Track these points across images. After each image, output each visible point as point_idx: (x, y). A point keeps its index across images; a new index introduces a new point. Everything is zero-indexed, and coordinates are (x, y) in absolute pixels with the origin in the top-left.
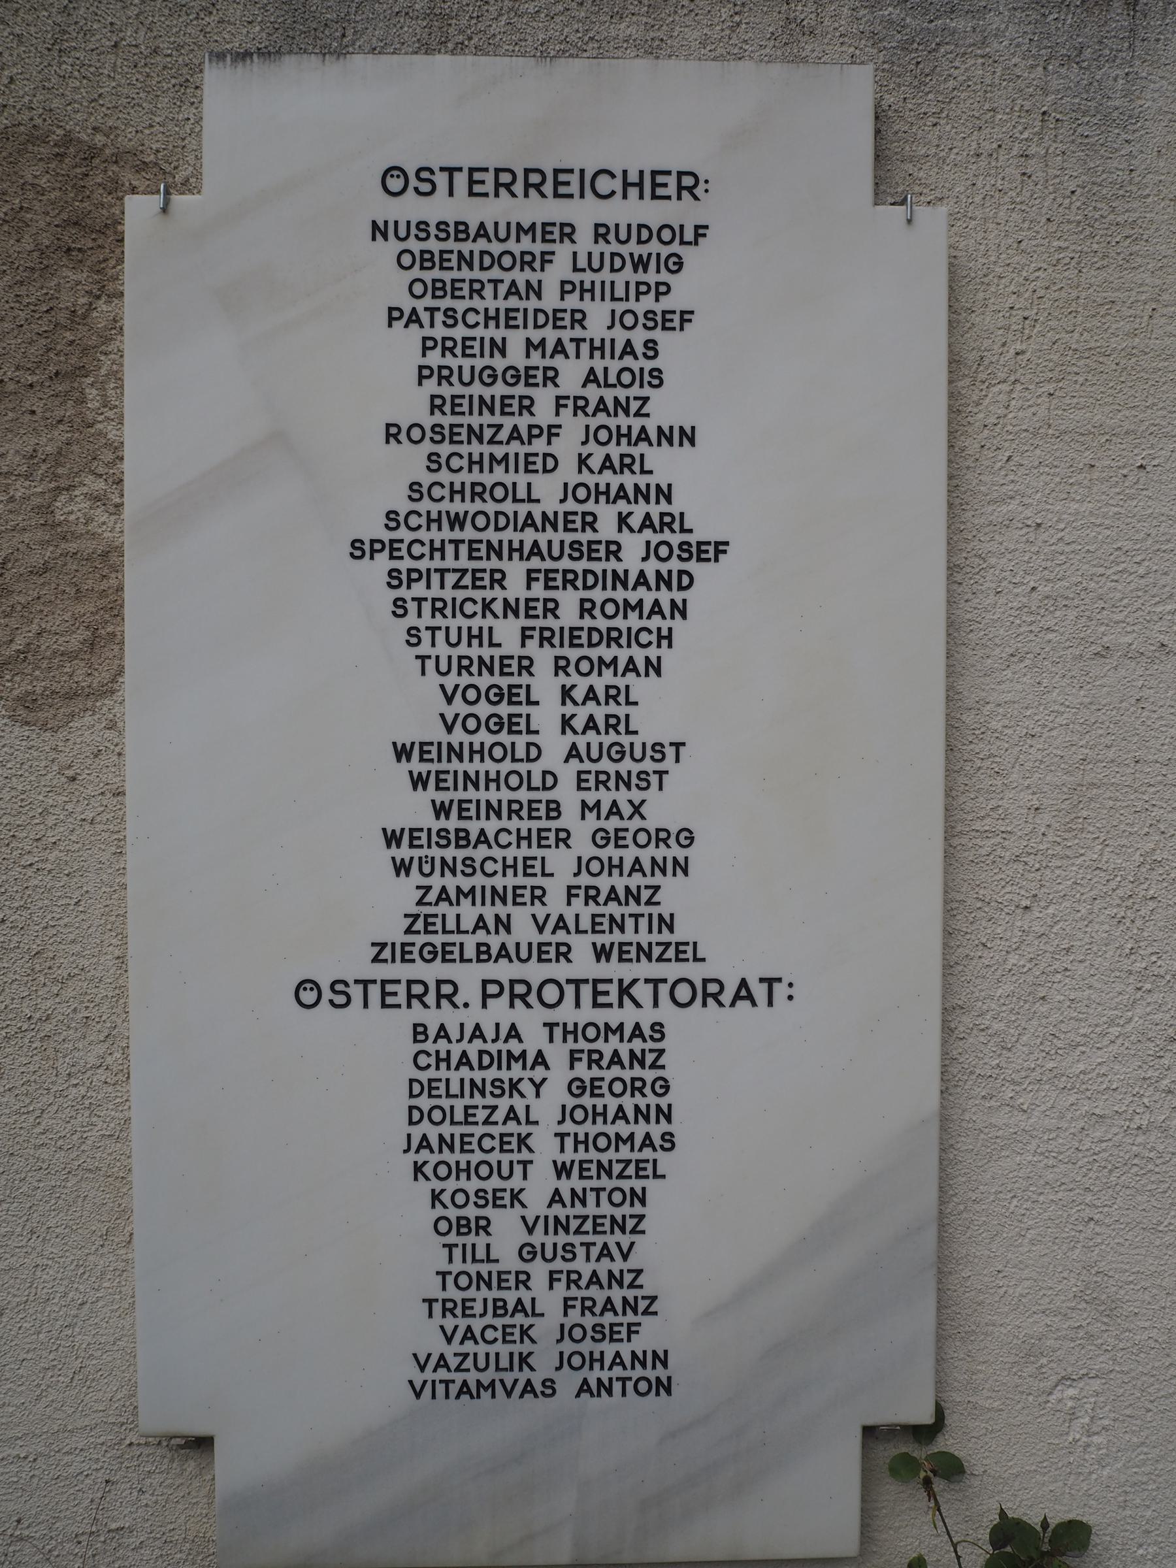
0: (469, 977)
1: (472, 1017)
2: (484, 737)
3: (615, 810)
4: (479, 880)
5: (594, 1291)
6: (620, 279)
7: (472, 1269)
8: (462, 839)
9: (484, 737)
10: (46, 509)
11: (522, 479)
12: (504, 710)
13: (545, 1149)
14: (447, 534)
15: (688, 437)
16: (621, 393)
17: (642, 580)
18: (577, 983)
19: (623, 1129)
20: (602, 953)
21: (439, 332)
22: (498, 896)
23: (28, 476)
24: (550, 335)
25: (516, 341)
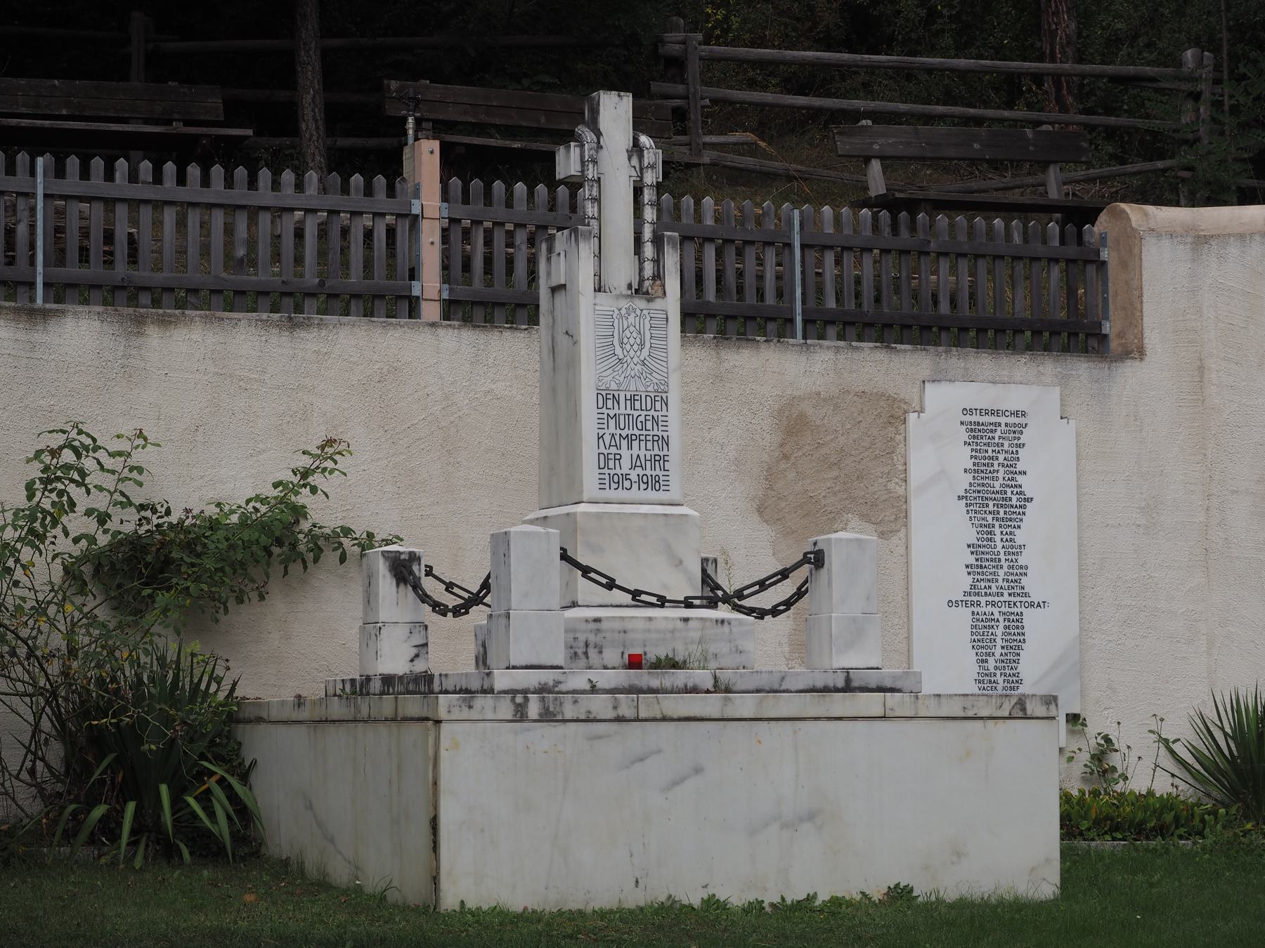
0: (983, 600)
1: (984, 609)
2: (985, 543)
3: (1012, 561)
4: (985, 577)
5: (1010, 678)
6: (1010, 436)
7: (984, 672)
8: (981, 566)
9: (985, 543)
10: (885, 486)
11: (992, 482)
12: (989, 536)
13: (999, 643)
14: (977, 495)
15: (1025, 473)
16: (1011, 463)
17: (1016, 506)
18: (1005, 602)
19: (1015, 637)
20: (1010, 595)
21: (975, 447)
22: (989, 581)
23: (882, 478)
24: (997, 448)
25: (990, 449)
